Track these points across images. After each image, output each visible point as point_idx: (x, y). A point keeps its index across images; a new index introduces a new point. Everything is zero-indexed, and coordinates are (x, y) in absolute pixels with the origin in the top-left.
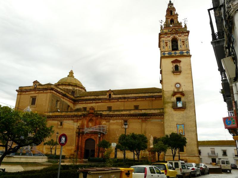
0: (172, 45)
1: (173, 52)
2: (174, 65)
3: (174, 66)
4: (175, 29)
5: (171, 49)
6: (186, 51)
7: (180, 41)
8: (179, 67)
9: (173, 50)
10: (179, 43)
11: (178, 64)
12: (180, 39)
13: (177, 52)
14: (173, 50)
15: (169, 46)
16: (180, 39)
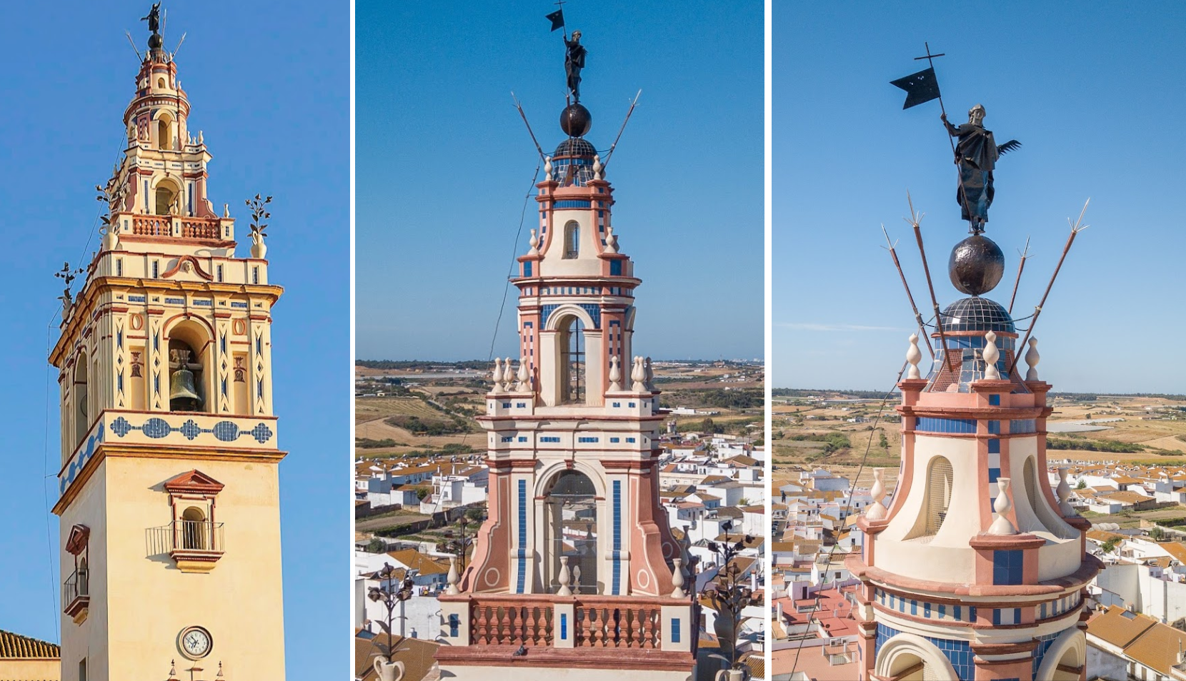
0: (172, 371)
1: (177, 421)
2: (182, 506)
3: (180, 513)
4: (194, 260)
5: (163, 400)
6: (257, 422)
7: (224, 348)
8: (207, 525)
9: (179, 405)
10: (220, 365)
11: (204, 506)
12: (224, 340)
13: (201, 421)
14: (179, 405)
15: (157, 380)
16: (224, 340)
